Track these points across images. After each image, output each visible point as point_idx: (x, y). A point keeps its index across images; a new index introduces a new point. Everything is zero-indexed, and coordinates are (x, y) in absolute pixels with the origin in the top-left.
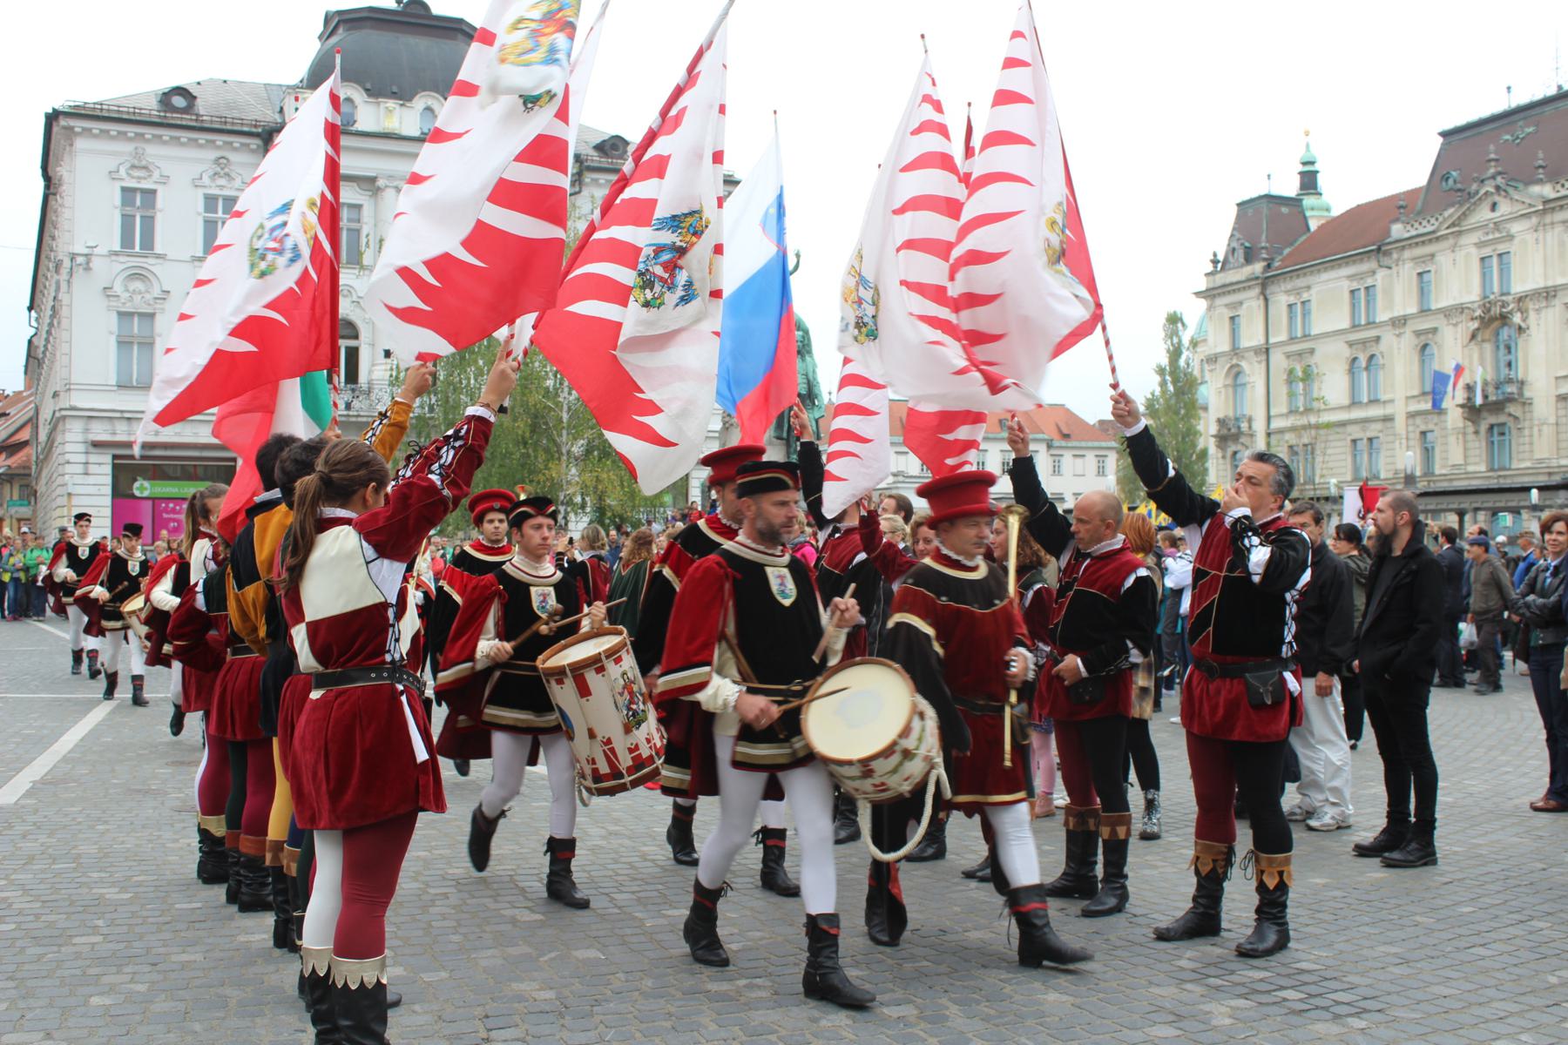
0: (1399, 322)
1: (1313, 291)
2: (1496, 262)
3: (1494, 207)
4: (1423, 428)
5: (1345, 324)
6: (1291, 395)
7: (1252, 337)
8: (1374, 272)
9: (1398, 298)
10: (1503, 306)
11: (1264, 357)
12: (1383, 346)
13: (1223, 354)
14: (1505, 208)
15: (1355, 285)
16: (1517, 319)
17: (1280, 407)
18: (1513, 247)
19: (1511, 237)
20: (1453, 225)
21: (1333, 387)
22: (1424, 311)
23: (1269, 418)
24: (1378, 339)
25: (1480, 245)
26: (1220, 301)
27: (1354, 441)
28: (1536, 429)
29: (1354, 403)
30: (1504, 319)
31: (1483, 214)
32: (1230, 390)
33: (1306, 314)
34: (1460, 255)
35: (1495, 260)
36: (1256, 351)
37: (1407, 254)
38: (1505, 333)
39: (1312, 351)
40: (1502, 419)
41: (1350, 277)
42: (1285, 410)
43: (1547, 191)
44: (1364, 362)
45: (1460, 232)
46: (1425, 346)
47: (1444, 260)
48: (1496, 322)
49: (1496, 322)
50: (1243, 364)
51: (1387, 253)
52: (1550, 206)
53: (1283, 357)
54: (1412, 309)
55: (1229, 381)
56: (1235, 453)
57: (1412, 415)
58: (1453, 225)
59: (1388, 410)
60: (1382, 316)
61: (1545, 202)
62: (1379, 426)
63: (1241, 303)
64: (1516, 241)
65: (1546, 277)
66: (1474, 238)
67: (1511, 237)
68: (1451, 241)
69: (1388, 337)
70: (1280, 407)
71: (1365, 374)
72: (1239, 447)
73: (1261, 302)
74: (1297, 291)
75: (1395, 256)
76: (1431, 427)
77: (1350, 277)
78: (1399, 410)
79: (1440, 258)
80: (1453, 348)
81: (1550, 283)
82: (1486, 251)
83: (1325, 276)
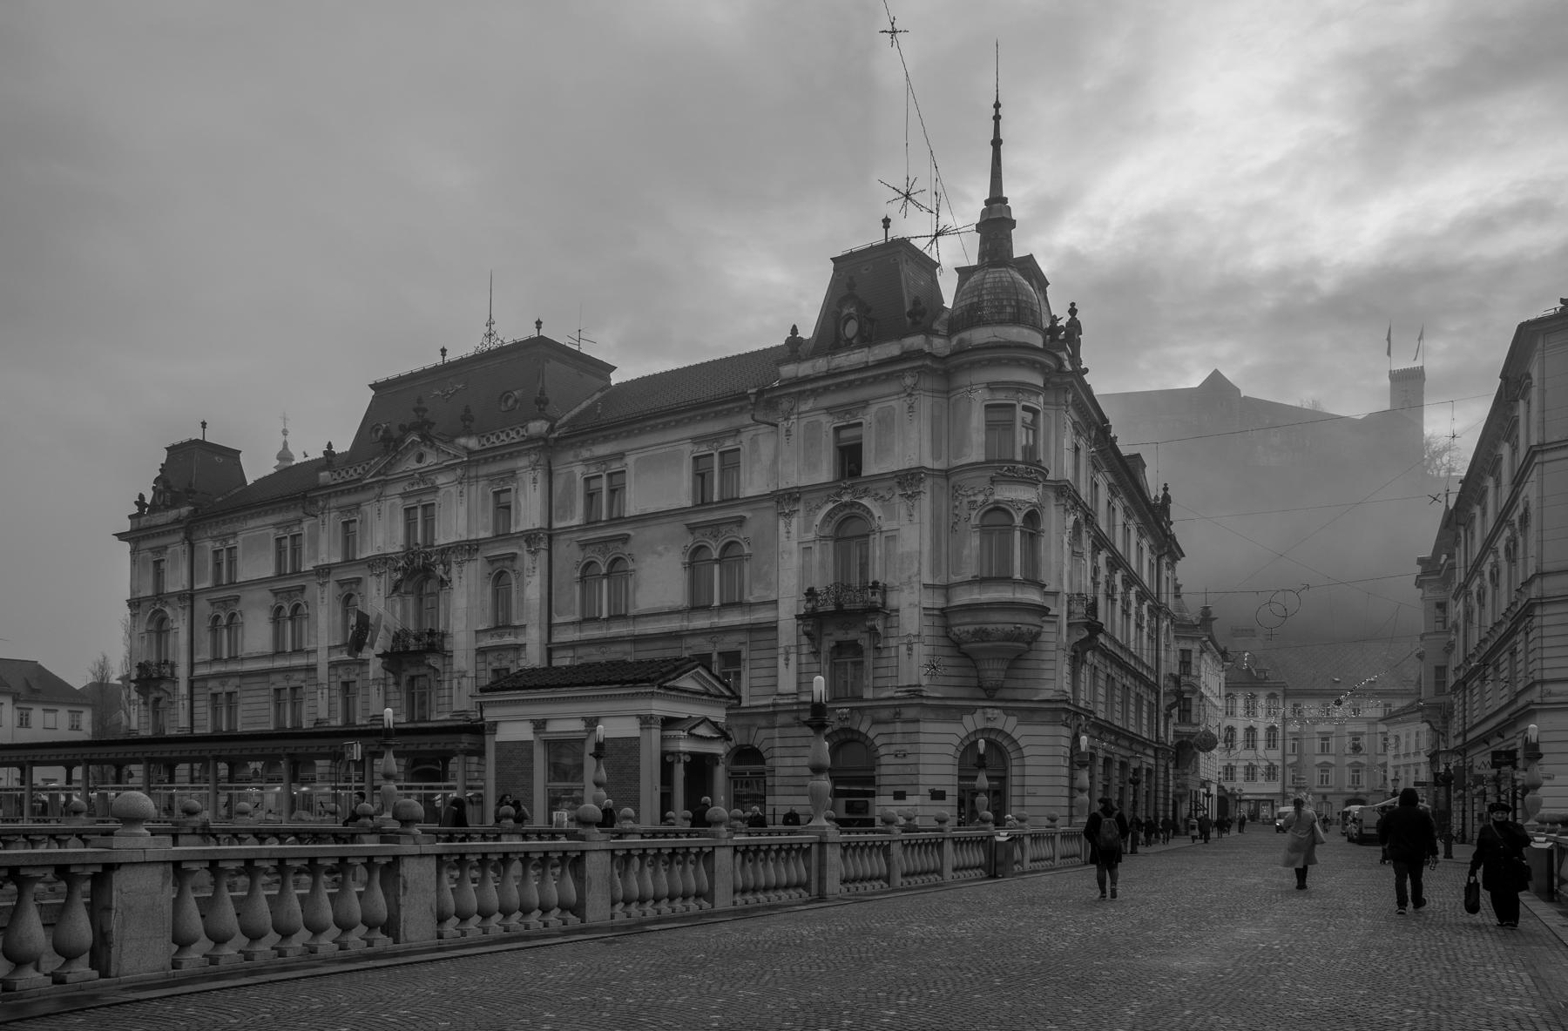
0: (323, 571)
1: (240, 538)
2: (420, 514)
3: (420, 458)
4: (345, 678)
5: (270, 572)
6: (216, 646)
7: (177, 580)
8: (301, 521)
9: (323, 546)
10: (426, 558)
11: (188, 603)
12: (307, 596)
13: (146, 598)
14: (431, 459)
15: (281, 533)
16: (440, 570)
17: (204, 654)
18: (439, 499)
19: (435, 489)
20: (378, 473)
21: (257, 635)
22: (349, 561)
23: (192, 666)
24: (302, 589)
25: (405, 495)
26: (144, 545)
27: (278, 691)
28: (455, 682)
29: (278, 653)
30: (427, 571)
31: (411, 464)
32: (154, 636)
33: (232, 562)
34: (385, 506)
35: (419, 511)
36: (180, 596)
37: (333, 503)
38: (430, 587)
39: (237, 599)
40: (423, 671)
41: (276, 525)
42: (208, 657)
43: (473, 443)
44: (289, 612)
45: (385, 483)
46: (349, 597)
47: (369, 510)
48: (420, 572)
49: (420, 572)
50: (168, 610)
51: (313, 501)
52: (475, 459)
53: (207, 604)
54: (337, 559)
55: (152, 627)
56: (158, 700)
57: (333, 665)
58: (378, 473)
59: (312, 660)
60: (307, 566)
61: (470, 452)
62: (302, 676)
63: (166, 547)
64: (441, 493)
65: (469, 532)
66: (399, 488)
67: (435, 489)
68: (377, 490)
69: (313, 589)
70: (204, 654)
71: (289, 623)
72: (161, 694)
73: (186, 547)
74: (223, 538)
75: (321, 504)
76: (352, 677)
77: (276, 525)
78: (322, 660)
79: (366, 508)
80: (376, 599)
81: (473, 537)
82: (411, 502)
83: (251, 523)
